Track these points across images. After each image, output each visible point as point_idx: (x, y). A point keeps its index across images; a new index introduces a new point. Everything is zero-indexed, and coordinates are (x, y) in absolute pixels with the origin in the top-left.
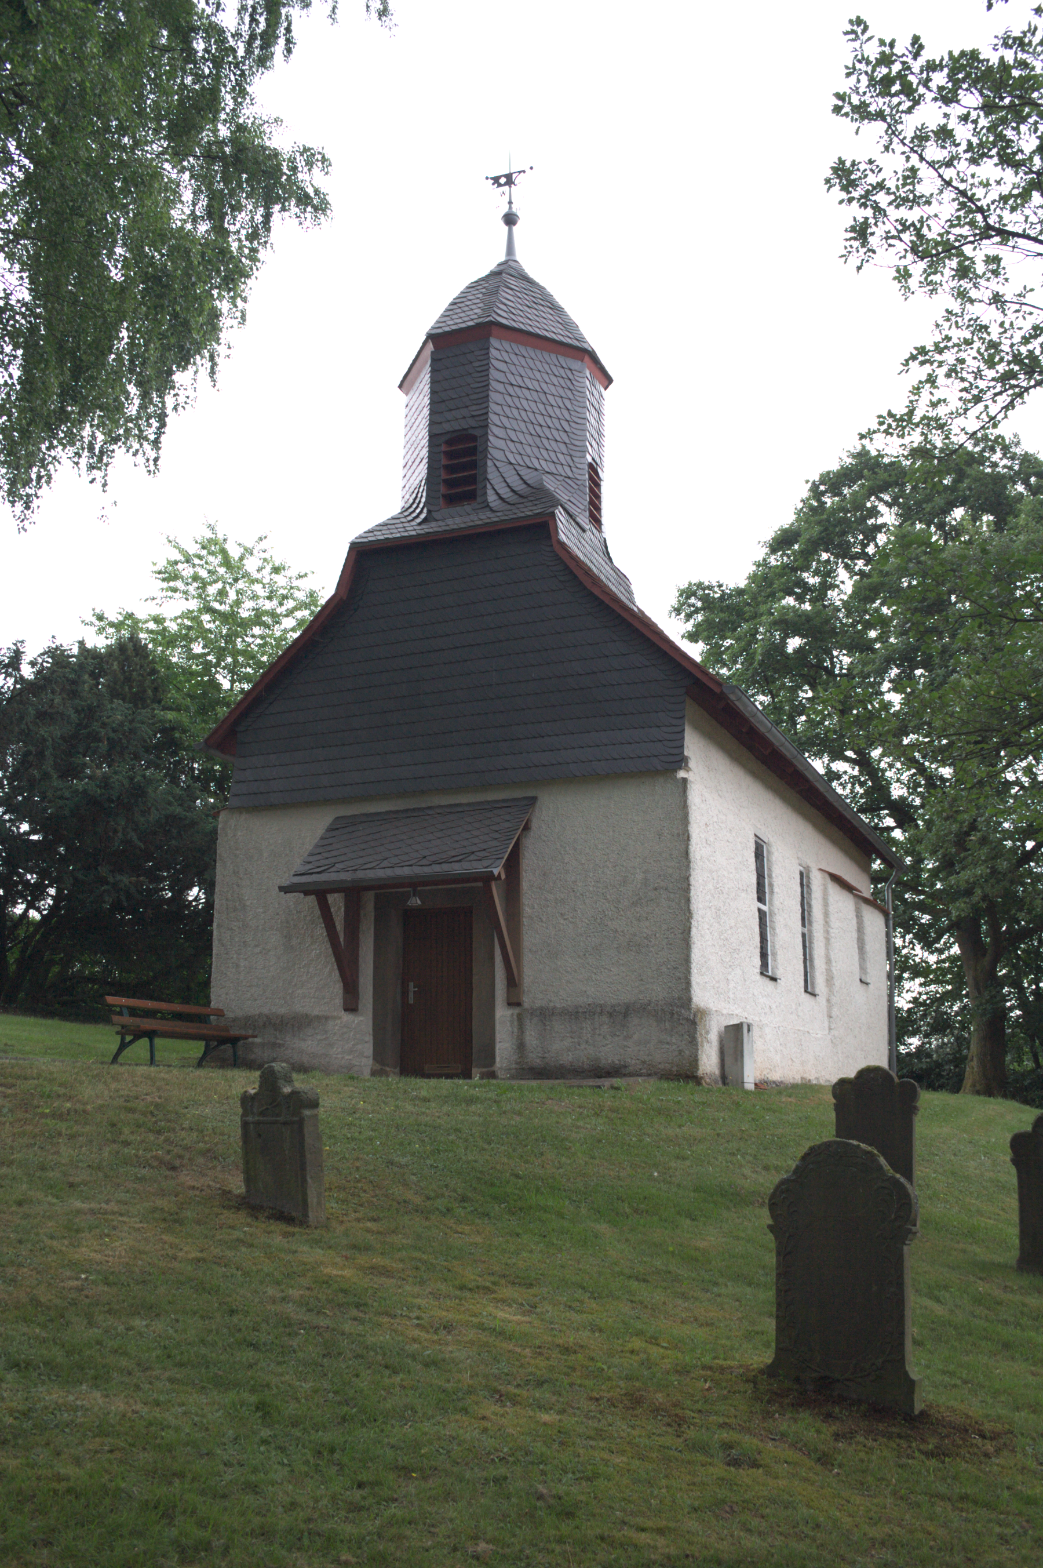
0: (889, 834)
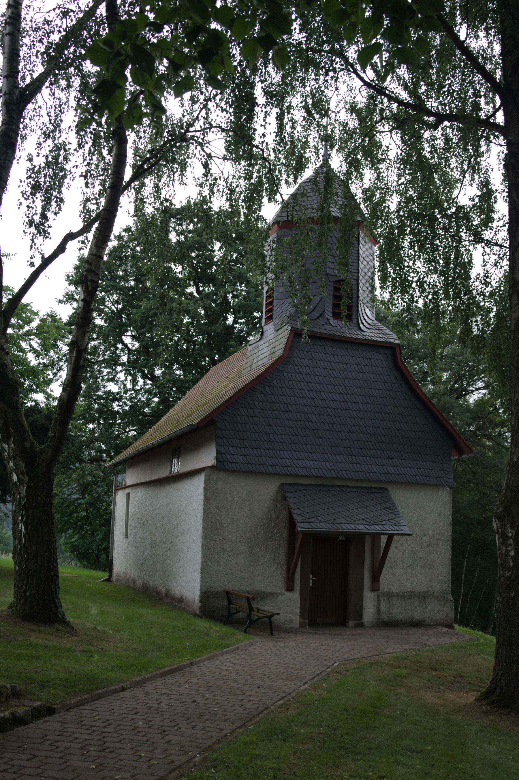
0: (421, 129)
